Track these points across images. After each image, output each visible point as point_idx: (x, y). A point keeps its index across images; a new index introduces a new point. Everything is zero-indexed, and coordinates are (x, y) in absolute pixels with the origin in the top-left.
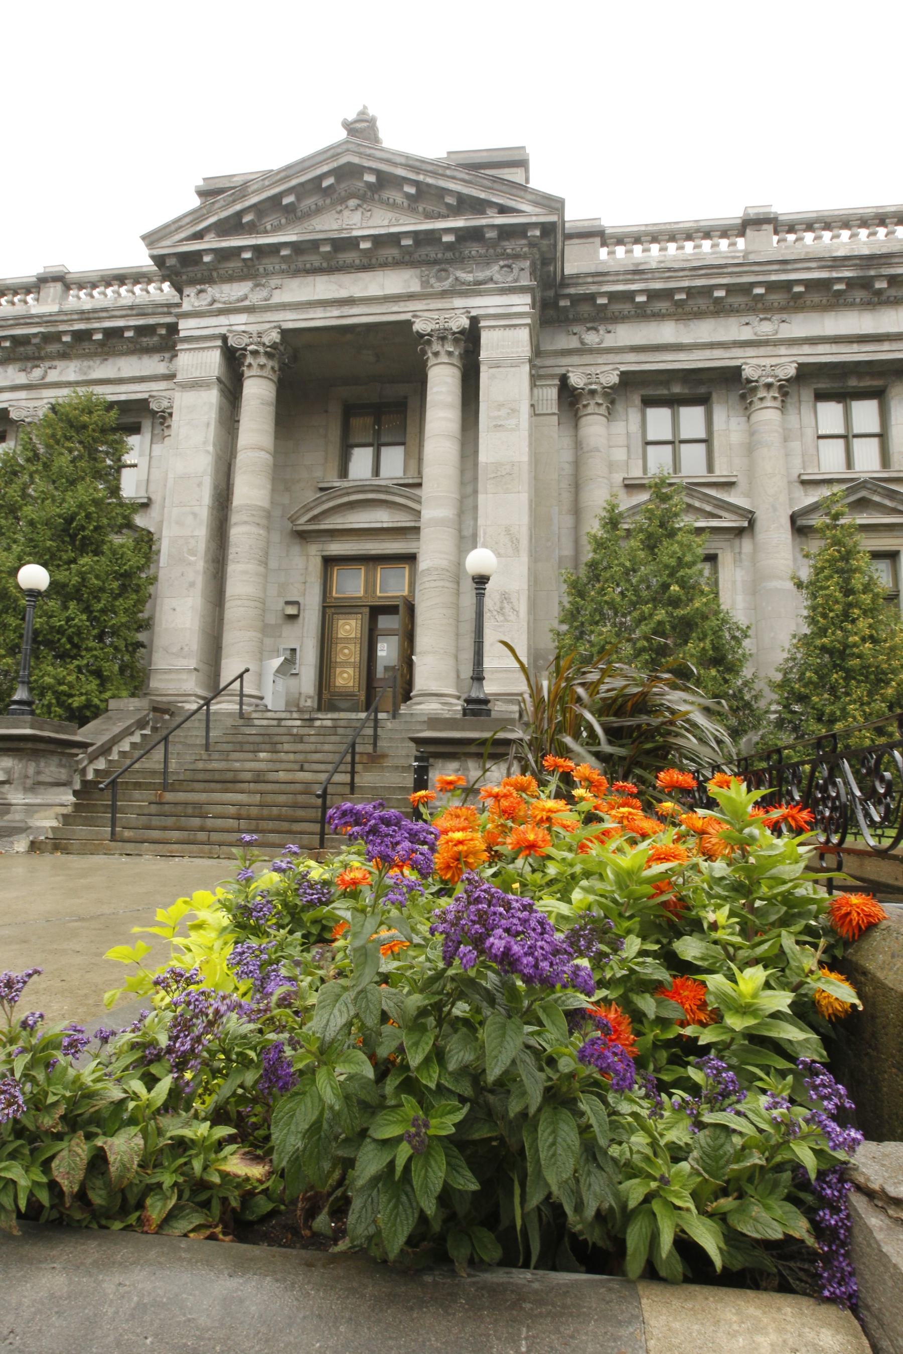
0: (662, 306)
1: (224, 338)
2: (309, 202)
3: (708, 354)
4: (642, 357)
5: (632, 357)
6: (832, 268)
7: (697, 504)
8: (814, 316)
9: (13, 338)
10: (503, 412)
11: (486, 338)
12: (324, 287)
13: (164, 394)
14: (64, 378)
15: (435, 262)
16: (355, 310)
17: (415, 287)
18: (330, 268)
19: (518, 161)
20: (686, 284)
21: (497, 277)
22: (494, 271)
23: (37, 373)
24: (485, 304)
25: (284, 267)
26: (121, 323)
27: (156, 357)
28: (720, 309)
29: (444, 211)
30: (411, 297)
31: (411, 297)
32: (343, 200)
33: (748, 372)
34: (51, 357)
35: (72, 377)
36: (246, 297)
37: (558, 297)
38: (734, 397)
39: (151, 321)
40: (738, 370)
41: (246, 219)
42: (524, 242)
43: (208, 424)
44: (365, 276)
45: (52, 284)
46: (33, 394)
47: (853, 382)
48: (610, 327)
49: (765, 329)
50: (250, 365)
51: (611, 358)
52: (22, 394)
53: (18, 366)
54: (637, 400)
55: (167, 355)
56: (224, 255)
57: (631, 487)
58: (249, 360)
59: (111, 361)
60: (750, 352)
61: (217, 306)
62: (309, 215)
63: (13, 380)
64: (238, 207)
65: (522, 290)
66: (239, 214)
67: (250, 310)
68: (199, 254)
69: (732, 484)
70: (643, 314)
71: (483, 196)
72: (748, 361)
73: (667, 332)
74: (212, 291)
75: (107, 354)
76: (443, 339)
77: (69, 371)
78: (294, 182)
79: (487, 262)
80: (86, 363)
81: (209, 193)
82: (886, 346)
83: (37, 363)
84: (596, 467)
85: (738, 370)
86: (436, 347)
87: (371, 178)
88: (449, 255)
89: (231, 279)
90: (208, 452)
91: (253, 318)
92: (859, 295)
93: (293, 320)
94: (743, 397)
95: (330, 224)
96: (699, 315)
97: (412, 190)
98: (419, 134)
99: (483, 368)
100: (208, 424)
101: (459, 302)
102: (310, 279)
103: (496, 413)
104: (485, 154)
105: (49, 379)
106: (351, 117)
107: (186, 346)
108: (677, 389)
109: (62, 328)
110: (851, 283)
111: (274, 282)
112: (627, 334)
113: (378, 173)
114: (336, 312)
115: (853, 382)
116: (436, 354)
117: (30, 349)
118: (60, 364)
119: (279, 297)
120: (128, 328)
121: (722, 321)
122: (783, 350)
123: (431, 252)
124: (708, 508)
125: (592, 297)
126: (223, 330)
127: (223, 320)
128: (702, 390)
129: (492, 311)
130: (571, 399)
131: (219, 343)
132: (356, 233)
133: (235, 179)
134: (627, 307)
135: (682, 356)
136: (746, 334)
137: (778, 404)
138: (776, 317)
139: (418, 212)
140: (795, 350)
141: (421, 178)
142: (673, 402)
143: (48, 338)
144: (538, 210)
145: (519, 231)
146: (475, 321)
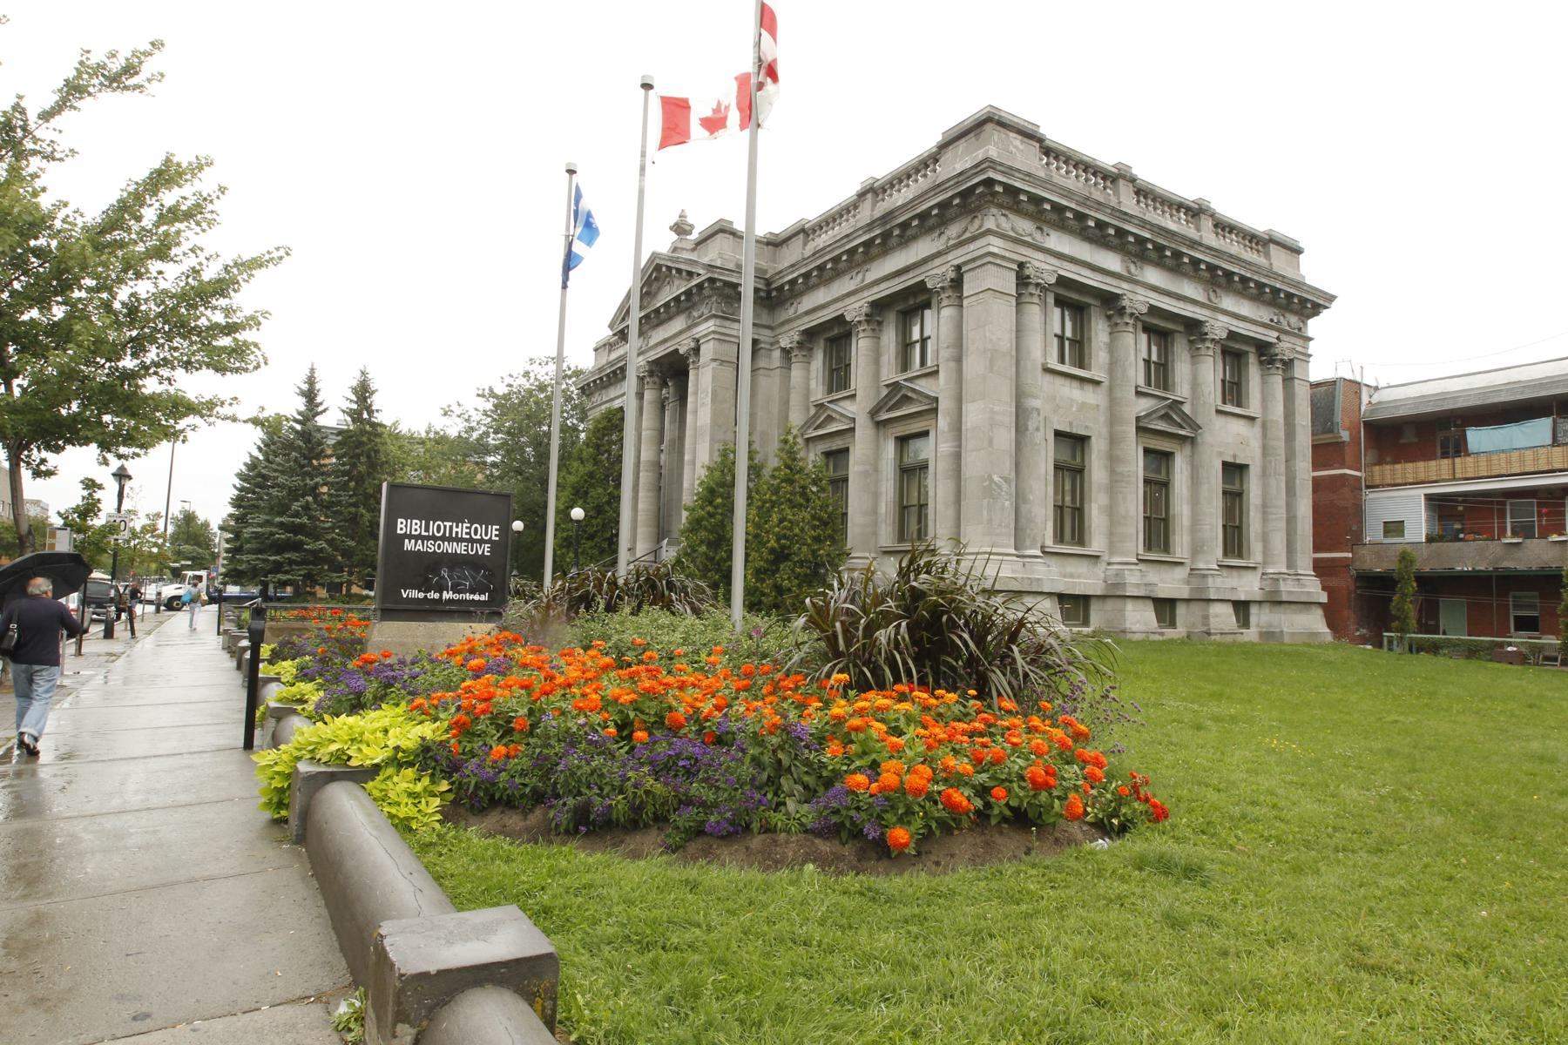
2: (655, 286)
5: (806, 319)
6: (870, 231)
11: (703, 348)
28: (837, 274)
31: (681, 333)
37: (769, 292)
40: (842, 316)
60: (852, 299)
82: (911, 275)
84: (795, 399)
93: (653, 355)
106: (675, 219)
125: (782, 286)
130: (786, 352)
135: (825, 312)
137: (869, 333)
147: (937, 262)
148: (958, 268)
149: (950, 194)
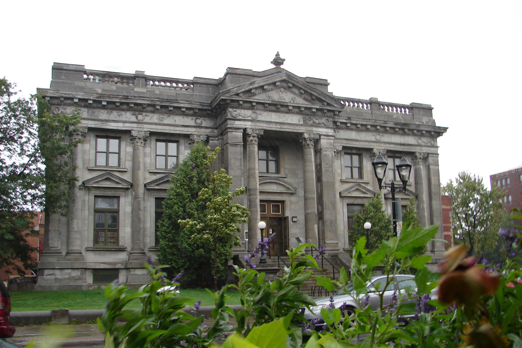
0: (353, 127)
1: (245, 130)
3: (364, 143)
4: (348, 142)
5: (344, 141)
7: (361, 189)
8: (389, 135)
9: (136, 104)
10: (328, 166)
12: (274, 117)
13: (194, 133)
14: (152, 121)
15: (308, 115)
16: (285, 127)
17: (302, 122)
18: (277, 111)
19: (325, 84)
20: (361, 123)
21: (325, 122)
22: (324, 120)
23: (140, 117)
24: (323, 131)
25: (263, 108)
26: (182, 105)
27: (190, 118)
28: (367, 130)
29: (310, 99)
30: (301, 125)
31: (301, 125)
32: (279, 88)
33: (375, 151)
34: (147, 112)
35: (156, 121)
36: (250, 116)
38: (368, 156)
39: (193, 106)
41: (253, 91)
42: (332, 114)
43: (241, 159)
44: (286, 115)
45: (141, 79)
46: (140, 126)
47: (397, 155)
48: (339, 131)
49: (378, 137)
50: (252, 140)
51: (339, 141)
52: (135, 125)
53: (131, 112)
54: (343, 153)
55: (194, 118)
56: (245, 102)
57: (342, 182)
58: (251, 138)
59: (171, 116)
60: (375, 144)
61: (240, 118)
62: (269, 91)
63: (130, 119)
64: (251, 87)
65: (332, 128)
66: (251, 90)
67: (252, 121)
68: (238, 101)
69: (368, 183)
70: (348, 128)
71: (324, 99)
72: (376, 147)
73: (353, 135)
74: (238, 111)
75: (170, 114)
76: (311, 140)
77: (155, 118)
78: (268, 82)
79: (321, 117)
80: (161, 116)
81: (231, 72)
82: (406, 147)
83: (141, 113)
85: (372, 149)
86: (308, 142)
87: (291, 85)
88: (312, 114)
89: (244, 109)
90: (241, 169)
91: (253, 124)
92: (401, 132)
94: (371, 156)
95: (276, 96)
96: (362, 131)
97: (303, 92)
98: (298, 67)
99: (322, 151)
100: (241, 159)
101: (314, 129)
102: (270, 113)
103: (326, 166)
104: (317, 80)
105: (145, 121)
107: (231, 130)
108: (354, 152)
109: (158, 103)
110: (399, 129)
111: (258, 112)
112: (343, 134)
113: (293, 85)
114: (279, 127)
115: (397, 155)
116: (308, 145)
117: (140, 107)
118: (151, 115)
119: (260, 118)
120: (183, 107)
121: (367, 133)
122: (382, 145)
123: (307, 112)
124: (364, 191)
126: (244, 127)
127: (242, 123)
128: (360, 152)
129: (323, 133)
131: (242, 131)
132: (289, 104)
133: (240, 70)
134: (344, 126)
135: (357, 143)
136: (373, 139)
138: (381, 134)
139: (302, 97)
140: (385, 145)
141: (306, 89)
142: (351, 154)
143: (149, 105)
144: (338, 107)
145: (333, 111)
146: (320, 135)
147: (418, 148)
148: (428, 154)
149: (432, 130)
